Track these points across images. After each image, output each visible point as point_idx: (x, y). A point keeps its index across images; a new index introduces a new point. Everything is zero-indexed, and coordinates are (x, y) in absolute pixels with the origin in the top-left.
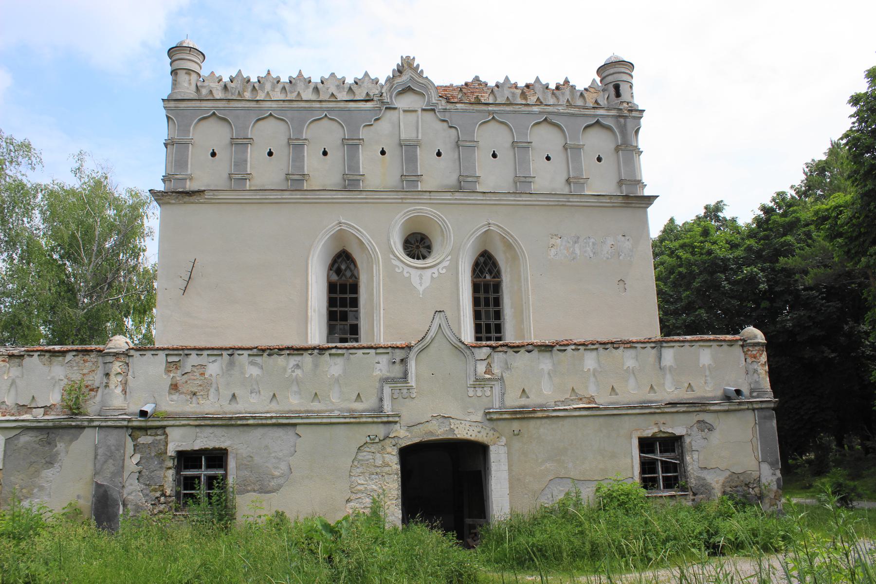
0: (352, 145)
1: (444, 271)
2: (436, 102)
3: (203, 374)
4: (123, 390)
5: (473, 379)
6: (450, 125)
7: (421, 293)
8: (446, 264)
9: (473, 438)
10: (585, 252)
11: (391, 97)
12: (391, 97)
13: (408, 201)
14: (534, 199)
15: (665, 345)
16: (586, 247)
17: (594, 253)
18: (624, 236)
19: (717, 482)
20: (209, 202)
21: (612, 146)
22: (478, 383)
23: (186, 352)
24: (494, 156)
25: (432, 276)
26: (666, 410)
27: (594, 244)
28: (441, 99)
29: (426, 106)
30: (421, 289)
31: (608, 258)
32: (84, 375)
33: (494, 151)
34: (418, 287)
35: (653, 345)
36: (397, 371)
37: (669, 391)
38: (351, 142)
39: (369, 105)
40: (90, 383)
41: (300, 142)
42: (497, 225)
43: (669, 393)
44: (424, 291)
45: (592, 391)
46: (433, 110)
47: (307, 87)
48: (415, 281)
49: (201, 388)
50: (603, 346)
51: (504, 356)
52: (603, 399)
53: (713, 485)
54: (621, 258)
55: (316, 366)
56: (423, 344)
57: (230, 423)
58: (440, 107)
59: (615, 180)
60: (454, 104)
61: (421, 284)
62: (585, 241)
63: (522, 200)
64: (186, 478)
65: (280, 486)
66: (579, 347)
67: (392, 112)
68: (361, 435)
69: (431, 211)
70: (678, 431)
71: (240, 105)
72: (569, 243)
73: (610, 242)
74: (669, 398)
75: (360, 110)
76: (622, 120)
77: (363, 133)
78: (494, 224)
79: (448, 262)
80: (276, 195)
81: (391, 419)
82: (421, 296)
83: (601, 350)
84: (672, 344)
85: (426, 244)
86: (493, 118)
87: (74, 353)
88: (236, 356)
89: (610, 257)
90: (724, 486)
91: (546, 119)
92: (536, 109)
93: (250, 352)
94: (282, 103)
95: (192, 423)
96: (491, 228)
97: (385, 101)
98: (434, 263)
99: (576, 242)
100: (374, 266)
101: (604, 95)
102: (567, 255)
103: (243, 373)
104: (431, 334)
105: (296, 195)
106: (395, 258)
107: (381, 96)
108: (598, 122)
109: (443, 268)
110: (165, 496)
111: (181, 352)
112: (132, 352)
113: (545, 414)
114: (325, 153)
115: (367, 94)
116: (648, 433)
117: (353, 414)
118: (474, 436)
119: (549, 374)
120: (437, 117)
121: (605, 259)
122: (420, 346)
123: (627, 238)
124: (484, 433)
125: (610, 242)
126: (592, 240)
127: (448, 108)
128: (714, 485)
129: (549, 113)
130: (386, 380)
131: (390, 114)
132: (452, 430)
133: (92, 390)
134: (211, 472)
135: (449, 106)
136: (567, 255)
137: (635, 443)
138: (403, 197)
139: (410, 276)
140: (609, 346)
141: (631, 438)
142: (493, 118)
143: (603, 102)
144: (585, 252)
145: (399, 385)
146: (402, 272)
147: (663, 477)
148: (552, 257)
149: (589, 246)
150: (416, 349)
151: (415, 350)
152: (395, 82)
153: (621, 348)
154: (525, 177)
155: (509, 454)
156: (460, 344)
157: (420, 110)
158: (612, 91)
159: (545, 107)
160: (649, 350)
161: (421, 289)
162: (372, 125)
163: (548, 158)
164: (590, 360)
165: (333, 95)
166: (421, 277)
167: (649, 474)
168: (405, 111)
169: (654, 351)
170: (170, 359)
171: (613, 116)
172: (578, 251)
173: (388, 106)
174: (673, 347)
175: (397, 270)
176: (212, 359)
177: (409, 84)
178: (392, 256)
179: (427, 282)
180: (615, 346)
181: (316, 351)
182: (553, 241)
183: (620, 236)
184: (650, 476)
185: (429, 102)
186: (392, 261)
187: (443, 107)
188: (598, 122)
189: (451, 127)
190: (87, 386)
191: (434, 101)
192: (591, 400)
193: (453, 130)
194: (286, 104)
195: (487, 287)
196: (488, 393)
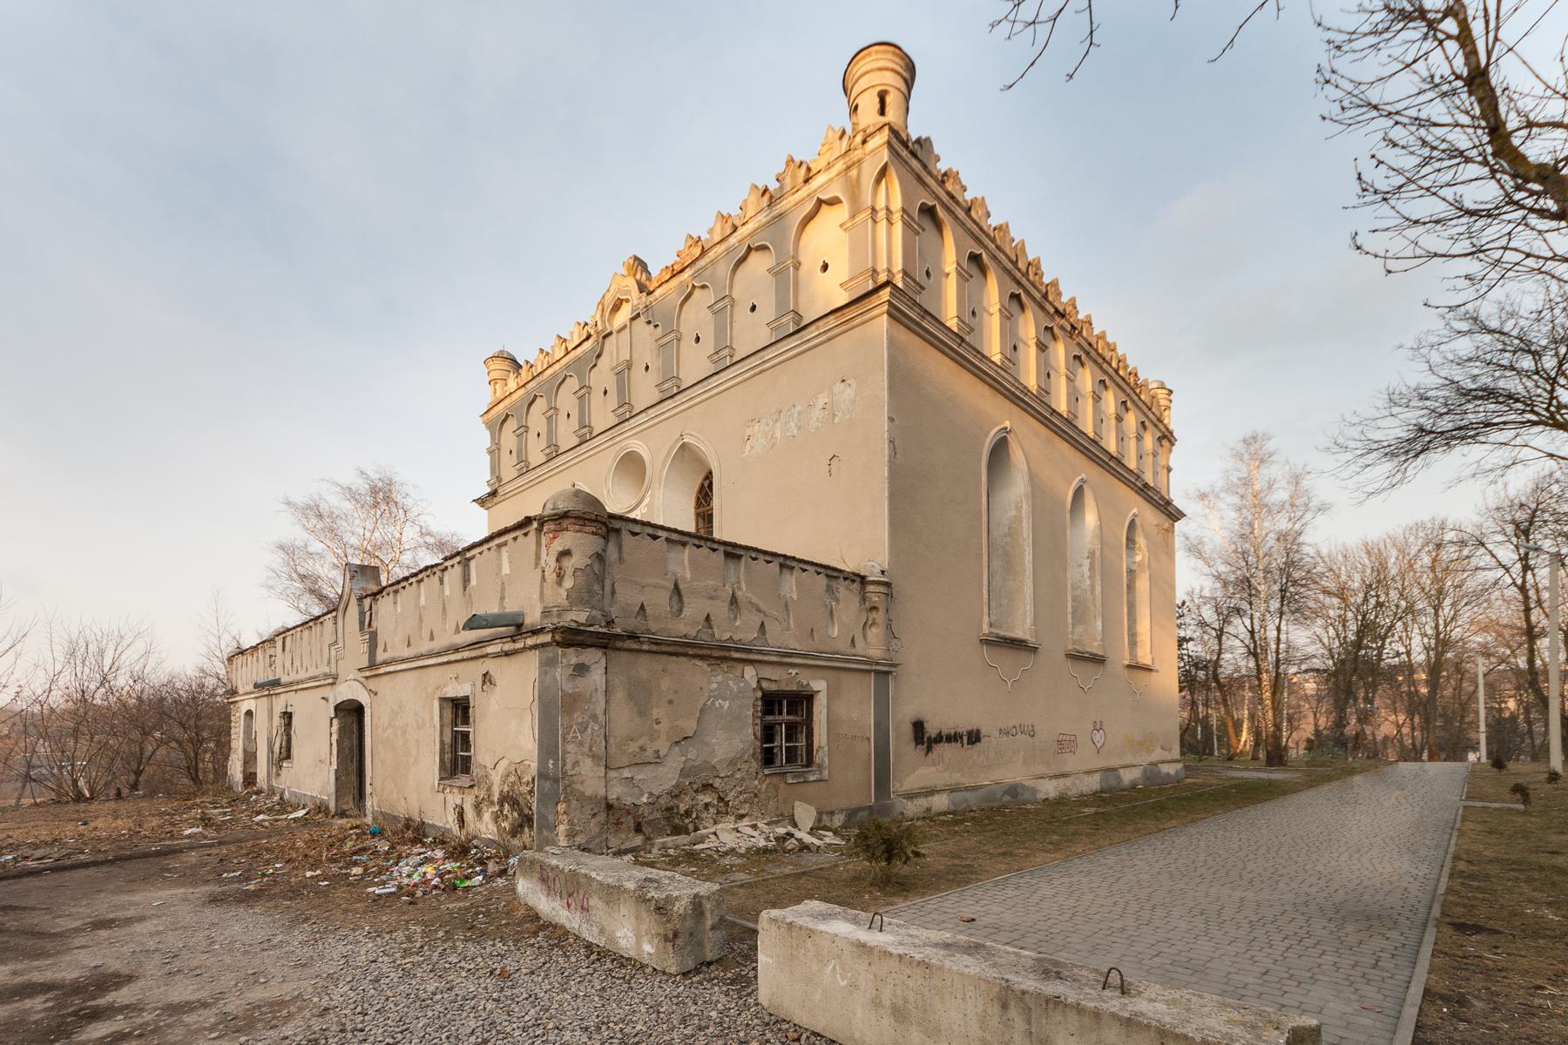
17: (799, 428)
18: (843, 381)
39: (590, 341)
54: (837, 420)
72: (768, 424)
73: (822, 399)
99: (777, 421)
126: (799, 408)
162: (595, 365)
168: (619, 331)
172: (778, 434)
183: (838, 384)
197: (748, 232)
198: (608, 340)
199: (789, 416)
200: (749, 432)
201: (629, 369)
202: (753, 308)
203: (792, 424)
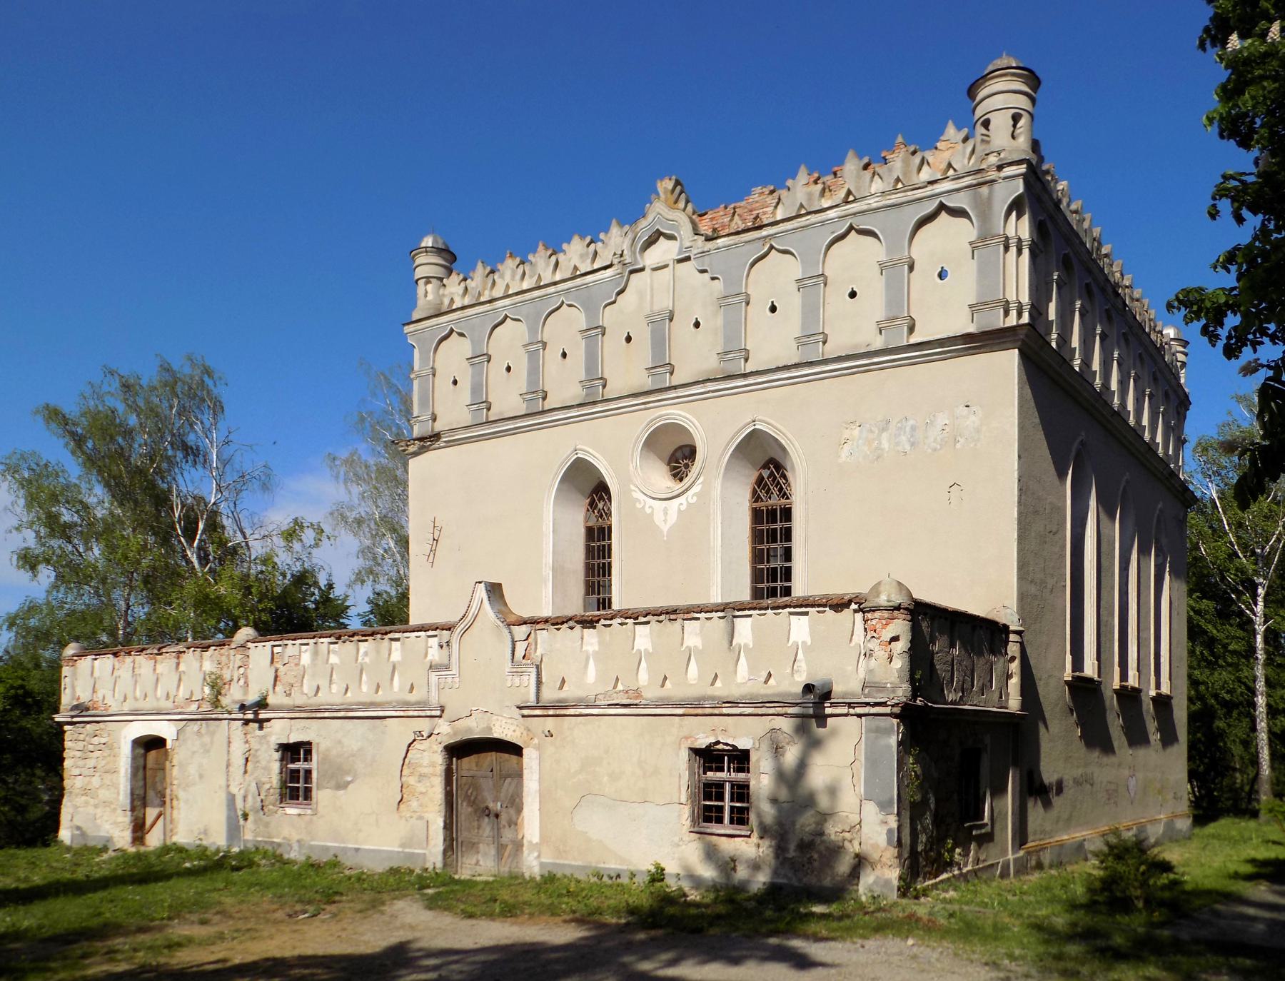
0: (595, 332)
4: (245, 683)
7: (665, 533)
9: (508, 739)
10: (898, 444)
11: (634, 253)
12: (634, 253)
14: (752, 382)
16: (900, 435)
17: (913, 444)
22: (515, 670)
24: (773, 309)
25: (679, 509)
26: (725, 711)
27: (913, 428)
29: (679, 254)
30: (665, 528)
31: (935, 450)
33: (772, 302)
35: (721, 614)
39: (609, 272)
43: (739, 685)
46: (688, 259)
47: (548, 265)
48: (658, 518)
50: (656, 618)
52: (651, 693)
55: (378, 652)
56: (465, 623)
57: (312, 713)
58: (696, 252)
61: (665, 521)
62: (899, 425)
65: (349, 783)
66: (628, 621)
68: (399, 731)
72: (872, 431)
74: (735, 692)
82: (665, 538)
83: (653, 623)
84: (747, 612)
88: (319, 644)
89: (939, 447)
96: (757, 427)
97: (627, 262)
98: (684, 488)
99: (884, 430)
102: (868, 453)
104: (473, 610)
106: (637, 489)
107: (621, 255)
109: (693, 495)
112: (250, 645)
116: (702, 742)
118: (509, 736)
121: (930, 451)
122: (462, 626)
124: (518, 733)
126: (911, 422)
127: (706, 249)
136: (868, 453)
137: (684, 755)
139: (653, 512)
140: (662, 617)
141: (680, 749)
144: (898, 444)
145: (443, 673)
146: (644, 507)
148: (844, 459)
149: (905, 432)
150: (459, 629)
151: (458, 630)
153: (679, 621)
160: (716, 620)
161: (665, 528)
162: (614, 302)
164: (644, 636)
166: (666, 511)
167: (716, 800)
168: (655, 269)
170: (277, 650)
172: (885, 445)
173: (631, 268)
174: (750, 616)
175: (638, 506)
176: (304, 648)
177: (658, 227)
178: (632, 487)
179: (673, 517)
180: (672, 617)
181: (379, 636)
182: (846, 434)
184: (716, 803)
186: (633, 493)
187: (700, 250)
189: (713, 279)
191: (688, 244)
194: (520, 298)
198: (633, 276)
199: (900, 429)
200: (846, 434)
201: (671, 320)
203: (904, 438)
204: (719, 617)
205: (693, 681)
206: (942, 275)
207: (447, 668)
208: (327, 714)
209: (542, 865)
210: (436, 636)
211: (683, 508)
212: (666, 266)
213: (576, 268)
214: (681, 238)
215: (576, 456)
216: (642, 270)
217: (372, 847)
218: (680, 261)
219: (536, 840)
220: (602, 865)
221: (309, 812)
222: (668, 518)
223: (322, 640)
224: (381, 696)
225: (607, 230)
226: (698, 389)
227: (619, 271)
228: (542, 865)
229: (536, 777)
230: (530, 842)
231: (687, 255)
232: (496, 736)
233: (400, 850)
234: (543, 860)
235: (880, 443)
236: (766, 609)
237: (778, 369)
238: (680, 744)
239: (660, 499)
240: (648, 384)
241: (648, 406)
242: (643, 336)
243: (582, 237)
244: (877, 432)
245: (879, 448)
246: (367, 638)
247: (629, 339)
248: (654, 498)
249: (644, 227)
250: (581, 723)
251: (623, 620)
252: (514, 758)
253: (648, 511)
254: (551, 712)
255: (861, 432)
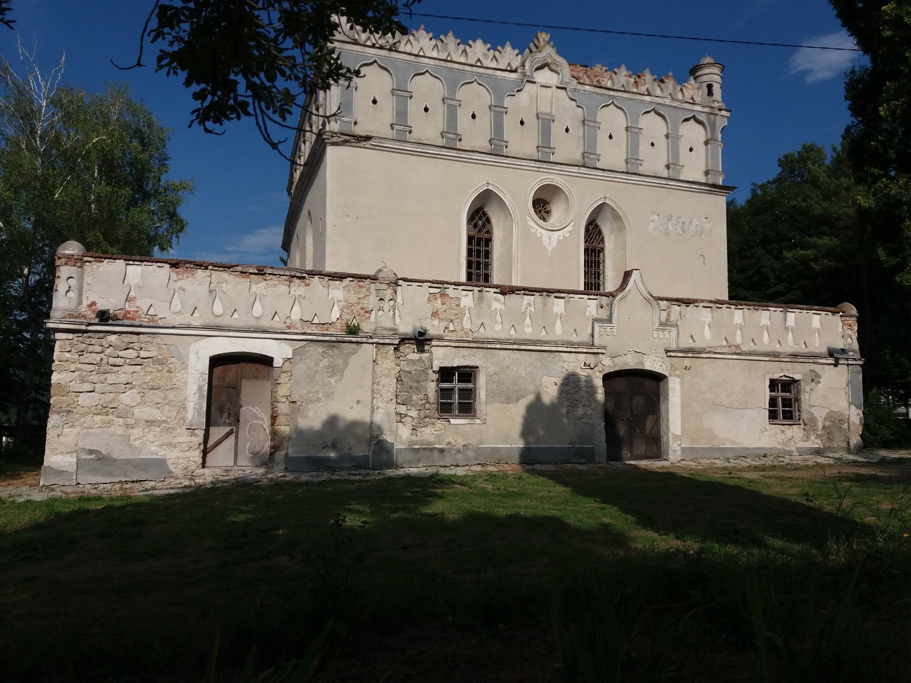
0: (498, 111)
1: (568, 235)
2: (569, 81)
3: (458, 305)
5: (658, 324)
6: (578, 104)
8: (569, 228)
9: (656, 370)
13: (542, 170)
15: (790, 310)
17: (683, 231)
19: (821, 417)
20: (374, 148)
21: (703, 139)
22: (661, 328)
23: (446, 286)
24: (611, 137)
25: (558, 239)
27: (683, 223)
28: (573, 79)
29: (560, 83)
30: (550, 248)
31: (693, 236)
32: (360, 298)
34: (547, 246)
35: (781, 309)
36: (604, 314)
37: (790, 344)
38: (497, 109)
39: (513, 75)
40: (365, 306)
41: (454, 103)
42: (611, 199)
44: (552, 250)
45: (739, 340)
46: (564, 89)
48: (545, 241)
49: (457, 317)
51: (679, 308)
53: (818, 419)
54: (703, 236)
55: (545, 305)
57: (482, 344)
58: (572, 87)
59: (703, 169)
60: (583, 85)
61: (550, 244)
63: (632, 180)
64: (442, 390)
66: (732, 306)
67: (531, 85)
69: (561, 182)
70: (797, 377)
71: (401, 57)
72: (664, 220)
75: (503, 78)
76: (712, 117)
77: (507, 102)
78: (609, 198)
79: (571, 228)
80: (435, 150)
81: (600, 351)
83: (746, 310)
85: (547, 210)
86: (613, 102)
87: (351, 279)
90: (825, 420)
91: (653, 109)
92: (647, 98)
93: (495, 290)
94: (438, 61)
95: (452, 344)
97: (527, 74)
99: (670, 220)
100: (514, 225)
101: (699, 92)
103: (490, 306)
105: (452, 153)
108: (694, 117)
110: (429, 403)
111: (441, 286)
112: (401, 282)
113: (708, 355)
114: (474, 116)
115: (509, 64)
117: (571, 344)
119: (709, 325)
120: (568, 95)
123: (709, 220)
125: (695, 222)
126: (682, 220)
128: (818, 418)
129: (658, 104)
130: (595, 320)
131: (529, 86)
132: (642, 363)
133: (366, 312)
134: (463, 385)
135: (579, 87)
137: (768, 383)
138: (539, 166)
139: (541, 237)
141: (765, 379)
142: (613, 102)
143: (698, 99)
144: (676, 229)
146: (536, 232)
147: (782, 410)
151: (618, 298)
152: (537, 57)
153: (760, 310)
154: (636, 160)
155: (682, 384)
156: (650, 297)
157: (554, 87)
158: (706, 91)
159: (655, 98)
161: (550, 248)
162: (514, 95)
163: (652, 144)
165: (479, 60)
166: (550, 238)
169: (782, 314)
171: (706, 112)
172: (670, 228)
173: (528, 79)
175: (531, 230)
178: (528, 218)
179: (554, 243)
180: (756, 308)
182: (652, 218)
185: (562, 79)
186: (529, 222)
188: (694, 117)
189: (578, 106)
190: (362, 309)
191: (567, 81)
192: (738, 347)
193: (580, 109)
195: (594, 250)
196: (668, 336)
197: (656, 101)
199: (676, 221)
200: (652, 218)
202: (652, 144)
203: (679, 227)
204: (781, 311)
205: (766, 342)
206: (691, 150)
207: (610, 320)
208: (498, 346)
209: (683, 449)
210: (596, 299)
211: (561, 238)
212: (550, 87)
213: (479, 60)
214: (562, 75)
215: (487, 188)
216: (534, 83)
217: (544, 446)
218: (558, 87)
219: (679, 433)
220: (722, 446)
221: (478, 421)
222: (551, 242)
223: (488, 289)
224: (543, 335)
225: (503, 47)
226: (575, 169)
227: (521, 77)
228: (683, 449)
229: (678, 394)
230: (673, 434)
231: (565, 86)
232: (647, 368)
233: (571, 446)
234: (683, 446)
235: (668, 227)
236: (803, 309)
237: (655, 177)
238: (765, 376)
239: (547, 230)
240: (535, 154)
241: (540, 170)
242: (532, 123)
243: (485, 43)
244: (666, 220)
245: (667, 229)
246: (535, 293)
247: (522, 123)
248: (543, 228)
249: (540, 57)
250: (707, 362)
251: (728, 306)
252: (654, 384)
253: (539, 235)
254: (690, 355)
255: (659, 218)
